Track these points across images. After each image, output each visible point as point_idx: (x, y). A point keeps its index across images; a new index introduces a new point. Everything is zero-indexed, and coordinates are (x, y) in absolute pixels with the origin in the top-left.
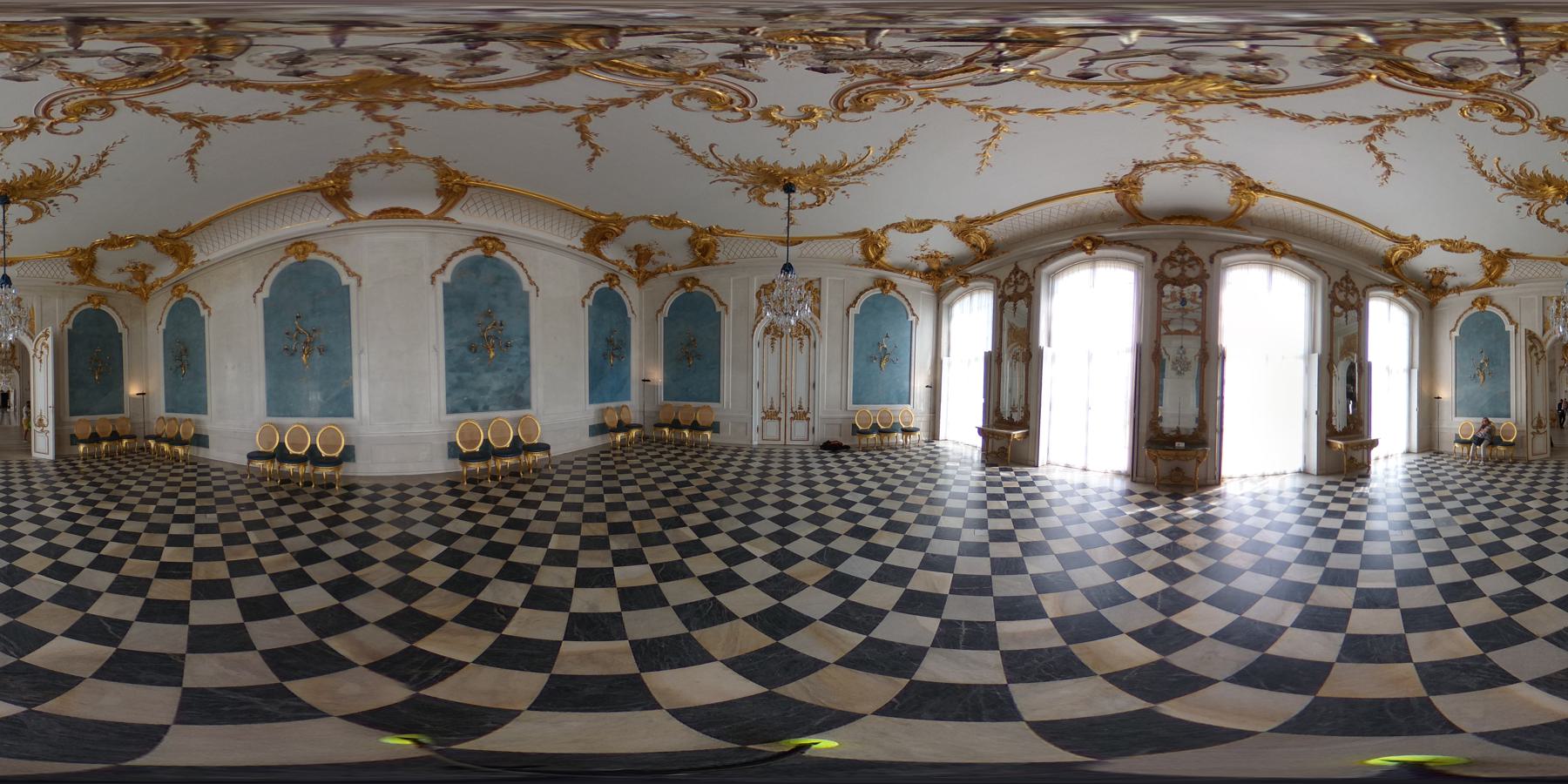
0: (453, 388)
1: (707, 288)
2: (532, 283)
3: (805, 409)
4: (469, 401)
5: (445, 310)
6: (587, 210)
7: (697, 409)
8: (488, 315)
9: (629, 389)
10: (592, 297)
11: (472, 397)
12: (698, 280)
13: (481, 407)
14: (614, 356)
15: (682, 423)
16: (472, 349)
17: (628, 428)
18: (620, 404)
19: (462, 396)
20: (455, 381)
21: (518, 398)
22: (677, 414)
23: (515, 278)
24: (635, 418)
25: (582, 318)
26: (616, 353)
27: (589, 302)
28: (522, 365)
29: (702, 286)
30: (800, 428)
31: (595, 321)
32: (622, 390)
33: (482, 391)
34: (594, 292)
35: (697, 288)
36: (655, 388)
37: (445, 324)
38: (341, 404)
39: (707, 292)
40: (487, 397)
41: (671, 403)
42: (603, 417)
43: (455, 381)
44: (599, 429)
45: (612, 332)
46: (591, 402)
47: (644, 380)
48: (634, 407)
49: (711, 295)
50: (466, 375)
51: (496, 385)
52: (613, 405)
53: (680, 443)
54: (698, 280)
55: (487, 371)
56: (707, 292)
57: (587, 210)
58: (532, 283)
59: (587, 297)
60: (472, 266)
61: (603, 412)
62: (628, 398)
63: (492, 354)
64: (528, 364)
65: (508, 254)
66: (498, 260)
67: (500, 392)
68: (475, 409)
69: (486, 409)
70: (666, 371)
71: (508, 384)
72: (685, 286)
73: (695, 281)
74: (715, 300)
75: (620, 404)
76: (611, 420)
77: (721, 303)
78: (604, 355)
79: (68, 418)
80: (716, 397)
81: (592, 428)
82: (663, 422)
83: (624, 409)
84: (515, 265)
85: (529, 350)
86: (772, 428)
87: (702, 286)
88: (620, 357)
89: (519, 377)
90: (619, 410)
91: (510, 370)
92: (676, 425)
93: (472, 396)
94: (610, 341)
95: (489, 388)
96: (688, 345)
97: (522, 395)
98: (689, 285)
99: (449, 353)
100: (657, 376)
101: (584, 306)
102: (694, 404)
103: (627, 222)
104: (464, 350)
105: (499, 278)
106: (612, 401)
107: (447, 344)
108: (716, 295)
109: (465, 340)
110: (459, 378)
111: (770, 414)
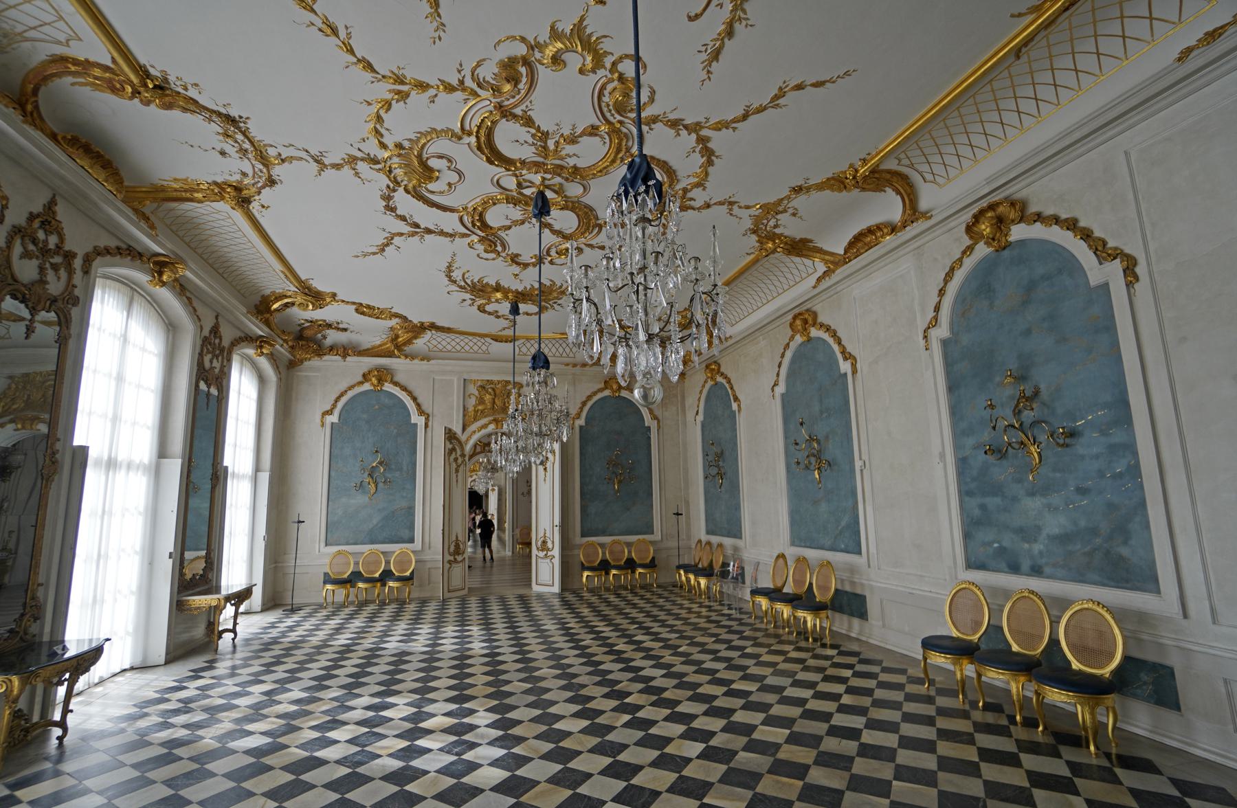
4: (1002, 551)
5: (952, 388)
11: (1006, 543)
16: (998, 452)
23: (1071, 265)
28: (1121, 475)
33: (1028, 533)
40: (1037, 547)
50: (993, 502)
51: (1054, 524)
55: (1032, 494)
66: (1022, 243)
67: (1064, 539)
68: (1015, 569)
69: (1036, 571)
71: (1083, 523)
79: (579, 540)
89: (1111, 506)
91: (1082, 491)
95: (1039, 529)
97: (1125, 551)
99: (962, 464)
105: (1031, 286)
107: (957, 447)
110: (983, 507)
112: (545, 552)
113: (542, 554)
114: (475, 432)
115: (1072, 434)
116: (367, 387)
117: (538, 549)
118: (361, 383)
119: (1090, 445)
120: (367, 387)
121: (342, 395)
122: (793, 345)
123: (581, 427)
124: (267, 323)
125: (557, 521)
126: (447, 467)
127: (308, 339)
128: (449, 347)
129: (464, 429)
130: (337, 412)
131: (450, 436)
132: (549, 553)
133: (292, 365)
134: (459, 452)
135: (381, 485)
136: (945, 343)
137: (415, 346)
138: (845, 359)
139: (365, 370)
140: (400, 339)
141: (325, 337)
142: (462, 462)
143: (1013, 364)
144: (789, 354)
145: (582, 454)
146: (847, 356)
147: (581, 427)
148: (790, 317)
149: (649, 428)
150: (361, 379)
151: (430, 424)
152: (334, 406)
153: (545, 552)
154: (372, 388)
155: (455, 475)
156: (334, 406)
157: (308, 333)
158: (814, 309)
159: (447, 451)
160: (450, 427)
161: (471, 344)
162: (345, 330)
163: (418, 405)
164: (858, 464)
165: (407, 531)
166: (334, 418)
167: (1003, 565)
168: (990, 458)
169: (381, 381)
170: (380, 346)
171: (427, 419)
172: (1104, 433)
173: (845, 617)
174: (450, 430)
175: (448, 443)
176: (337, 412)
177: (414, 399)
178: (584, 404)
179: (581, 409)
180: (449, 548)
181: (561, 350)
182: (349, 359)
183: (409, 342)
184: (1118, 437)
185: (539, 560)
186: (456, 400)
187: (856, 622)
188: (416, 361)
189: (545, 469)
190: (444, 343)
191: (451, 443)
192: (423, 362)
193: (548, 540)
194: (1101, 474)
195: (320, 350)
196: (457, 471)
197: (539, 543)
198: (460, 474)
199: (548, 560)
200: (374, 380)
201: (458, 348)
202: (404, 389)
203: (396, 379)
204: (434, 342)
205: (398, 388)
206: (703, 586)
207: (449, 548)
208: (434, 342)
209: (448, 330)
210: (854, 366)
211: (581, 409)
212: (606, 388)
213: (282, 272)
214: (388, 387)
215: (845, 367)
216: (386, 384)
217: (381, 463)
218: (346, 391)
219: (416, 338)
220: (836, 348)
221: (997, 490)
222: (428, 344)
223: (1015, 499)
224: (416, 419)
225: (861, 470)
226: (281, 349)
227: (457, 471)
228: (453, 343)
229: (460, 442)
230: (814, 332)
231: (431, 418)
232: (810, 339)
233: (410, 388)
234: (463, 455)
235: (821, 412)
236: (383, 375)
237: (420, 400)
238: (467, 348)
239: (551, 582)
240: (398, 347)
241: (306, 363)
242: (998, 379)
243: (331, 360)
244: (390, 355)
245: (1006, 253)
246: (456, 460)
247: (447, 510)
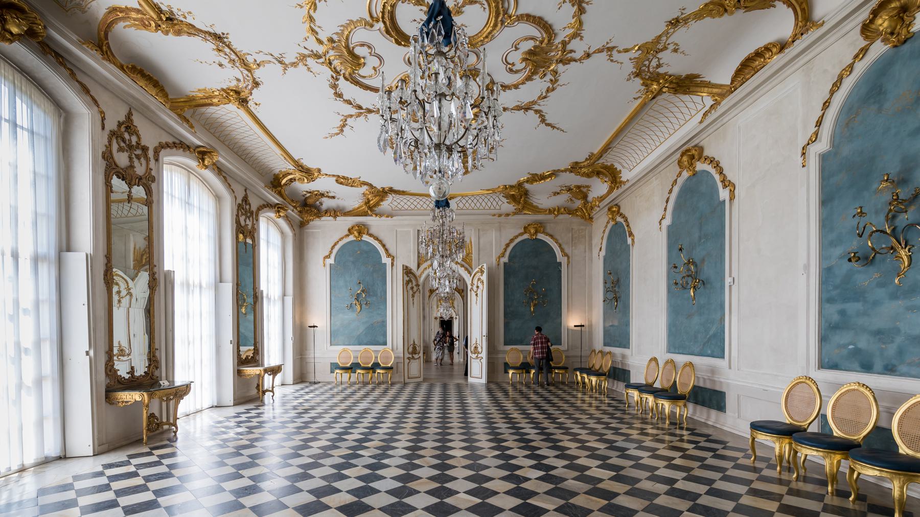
13: (878, 364)
20: (836, 318)
43: (836, 318)
50: (853, 307)
55: (894, 296)
93: (863, 343)
110: (842, 313)
112: (476, 355)
113: (474, 356)
114: (426, 269)
116: (351, 238)
117: (471, 352)
118: (347, 236)
120: (351, 238)
121: (335, 244)
122: (680, 181)
123: (505, 264)
124: (280, 194)
125: (485, 333)
126: (405, 293)
127: (311, 206)
128: (406, 207)
129: (419, 266)
130: (333, 256)
131: (407, 271)
132: (479, 355)
133: (302, 225)
134: (414, 283)
135: (364, 306)
137: (382, 206)
138: (725, 187)
139: (350, 226)
140: (371, 202)
141: (321, 204)
142: (417, 290)
144: (676, 189)
145: (505, 284)
146: (726, 183)
147: (505, 264)
148: (678, 155)
149: (560, 264)
150: (347, 233)
151: (395, 263)
152: (331, 252)
153: (476, 355)
154: (355, 239)
155: (411, 299)
156: (331, 252)
157: (310, 201)
158: (701, 144)
159: (405, 282)
160: (408, 265)
161: (421, 203)
162: (334, 197)
163: (386, 250)
164: (728, 280)
165: (382, 337)
166: (331, 261)
168: (855, 265)
169: (360, 233)
170: (358, 208)
171: (393, 260)
173: (705, 409)
174: (407, 267)
175: (405, 276)
176: (333, 256)
177: (384, 246)
178: (508, 245)
179: (505, 250)
180: (408, 349)
181: (489, 204)
182: (338, 218)
183: (377, 204)
185: (473, 360)
186: (412, 246)
187: (714, 413)
188: (383, 218)
189: (477, 295)
190: (402, 203)
191: (408, 276)
192: (388, 218)
193: (479, 346)
195: (319, 212)
196: (413, 296)
197: (473, 348)
198: (415, 298)
199: (479, 360)
200: (356, 234)
201: (413, 206)
202: (377, 239)
203: (371, 232)
204: (396, 204)
205: (372, 238)
206: (594, 383)
207: (408, 349)
208: (396, 204)
209: (403, 193)
210: (732, 193)
211: (505, 250)
212: (525, 232)
213: (282, 155)
214: (365, 238)
215: (724, 194)
216: (364, 236)
217: (363, 291)
218: (338, 242)
219: (382, 200)
220: (717, 177)
221: (858, 295)
222: (391, 204)
223: (876, 303)
224: (386, 260)
225: (730, 286)
226: (293, 213)
227: (413, 296)
228: (409, 203)
229: (415, 276)
230: (700, 166)
231: (395, 259)
232: (695, 174)
233: (381, 238)
234: (418, 285)
235: (700, 238)
236: (361, 229)
237: (388, 246)
238: (419, 206)
239: (480, 376)
240: (370, 208)
241: (311, 223)
243: (327, 221)
244: (365, 214)
246: (412, 288)
247: (406, 323)
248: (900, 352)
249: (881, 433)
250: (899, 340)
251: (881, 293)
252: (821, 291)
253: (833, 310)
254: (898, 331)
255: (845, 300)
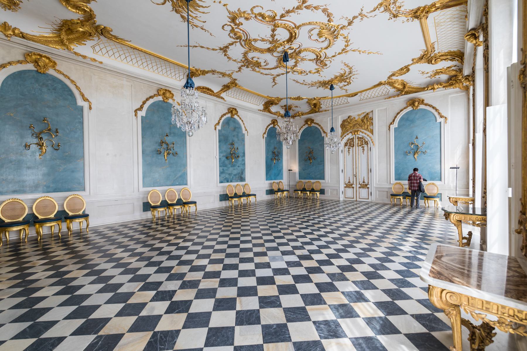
0: (221, 173)
1: (317, 124)
2: (246, 130)
3: (366, 183)
5: (220, 141)
6: (268, 96)
7: (314, 183)
8: (232, 144)
9: (282, 174)
10: (266, 133)
12: (313, 120)
13: (229, 181)
14: (275, 159)
15: (307, 189)
16: (227, 158)
17: (283, 191)
18: (278, 181)
19: (224, 178)
20: (222, 170)
21: (242, 179)
22: (304, 185)
23: (240, 128)
24: (286, 188)
25: (263, 143)
26: (276, 158)
27: (265, 136)
28: (243, 164)
29: (315, 123)
30: (364, 193)
31: (268, 144)
32: (279, 174)
33: (230, 174)
34: (267, 130)
35: (313, 125)
36: (295, 173)
37: (219, 148)
38: (182, 180)
39: (317, 126)
41: (302, 180)
42: (272, 187)
44: (271, 192)
45: (275, 148)
46: (267, 180)
47: (289, 170)
48: (285, 182)
49: (319, 128)
50: (225, 168)
51: (235, 172)
52: (276, 181)
53: (306, 199)
54: (313, 120)
55: (231, 167)
56: (317, 126)
57: (268, 96)
58: (246, 130)
59: (265, 133)
60: (227, 122)
61: (271, 184)
62: (282, 179)
63: (233, 160)
64: (244, 164)
65: (238, 116)
66: (235, 119)
67: (235, 175)
68: (228, 182)
69: (231, 181)
70: (300, 165)
72: (307, 123)
73: (312, 121)
74: (321, 130)
75: (278, 181)
76: (275, 188)
77: (324, 132)
78: (272, 159)
80: (322, 177)
81: (267, 191)
82: (298, 189)
83: (280, 183)
84: (240, 121)
85: (245, 158)
86: (349, 192)
87: (315, 123)
88: (278, 160)
89: (242, 169)
90: (278, 183)
91: (239, 167)
92: (304, 190)
93: (227, 176)
94: (274, 153)
96: (310, 153)
97: (242, 176)
98: (309, 123)
99: (220, 159)
100: (296, 168)
101: (263, 138)
102: (312, 181)
103: (282, 99)
104: (224, 158)
106: (275, 179)
107: (219, 156)
108: (322, 128)
109: (225, 154)
110: (223, 169)
111: (349, 185)
115: (238, 157)
119: (240, 159)
136: (219, 130)
143: (231, 141)
167: (226, 181)
172: (242, 157)
184: (243, 158)
194: (241, 164)
221: (226, 166)
223: (229, 168)
242: (228, 143)
245: (232, 119)
248: (233, 178)
249: (236, 194)
250: (232, 175)
251: (229, 166)
252: (219, 164)
253: (222, 168)
254: (232, 173)
255: (224, 167)
